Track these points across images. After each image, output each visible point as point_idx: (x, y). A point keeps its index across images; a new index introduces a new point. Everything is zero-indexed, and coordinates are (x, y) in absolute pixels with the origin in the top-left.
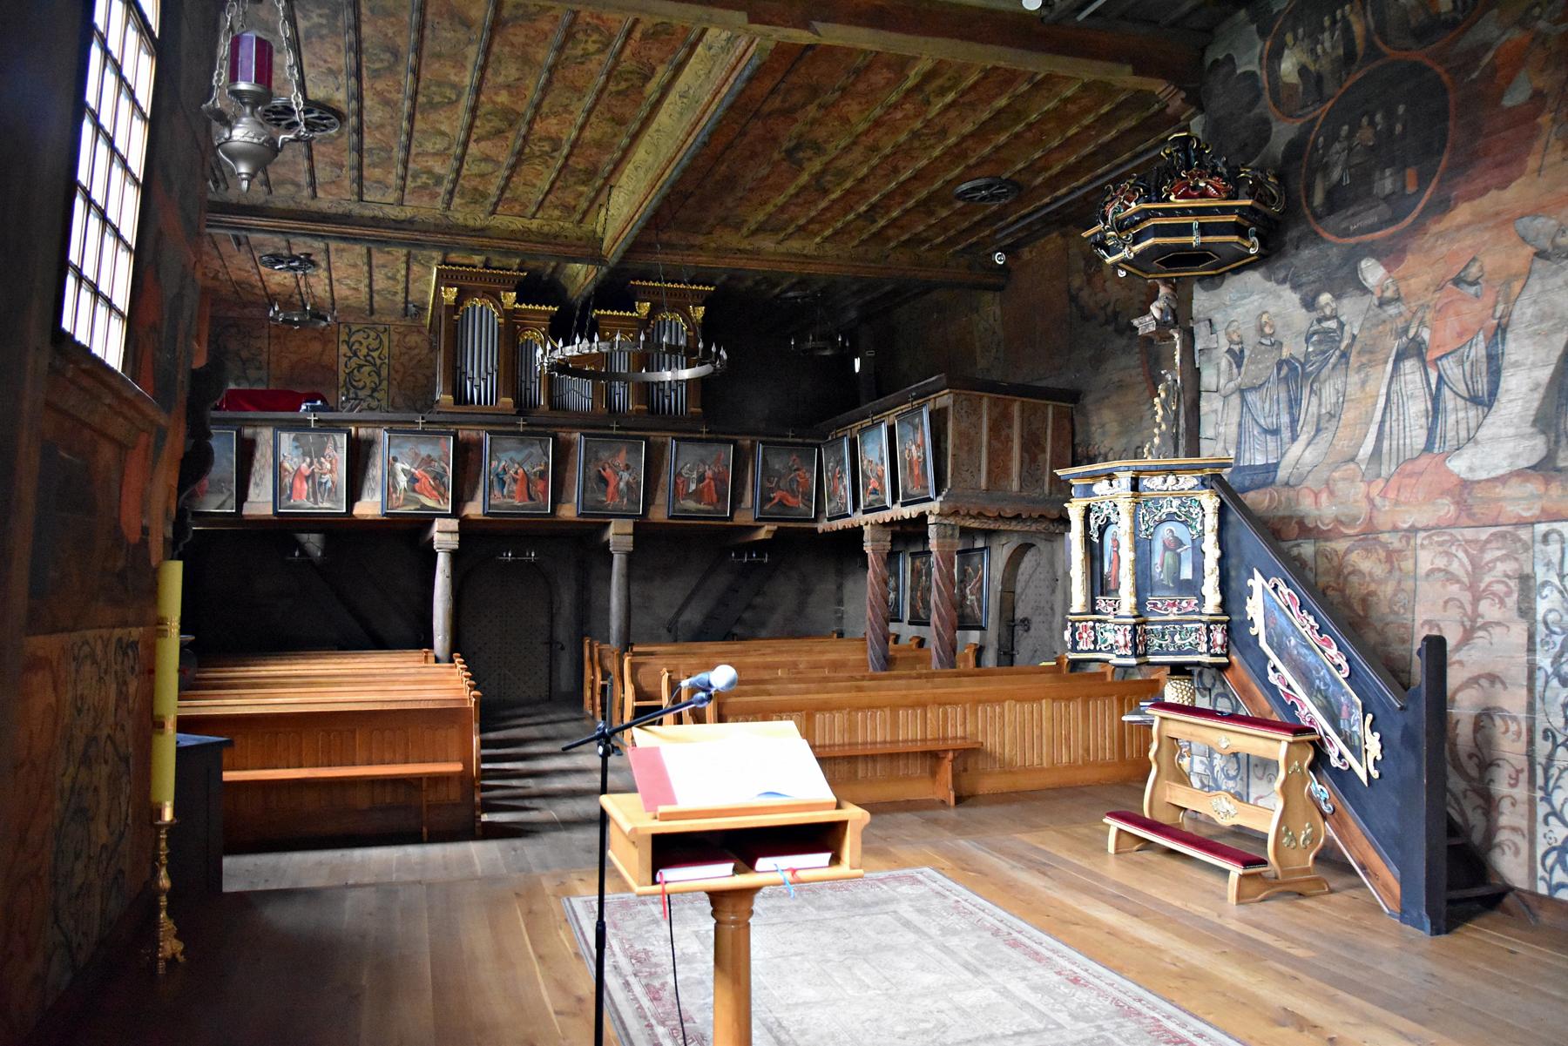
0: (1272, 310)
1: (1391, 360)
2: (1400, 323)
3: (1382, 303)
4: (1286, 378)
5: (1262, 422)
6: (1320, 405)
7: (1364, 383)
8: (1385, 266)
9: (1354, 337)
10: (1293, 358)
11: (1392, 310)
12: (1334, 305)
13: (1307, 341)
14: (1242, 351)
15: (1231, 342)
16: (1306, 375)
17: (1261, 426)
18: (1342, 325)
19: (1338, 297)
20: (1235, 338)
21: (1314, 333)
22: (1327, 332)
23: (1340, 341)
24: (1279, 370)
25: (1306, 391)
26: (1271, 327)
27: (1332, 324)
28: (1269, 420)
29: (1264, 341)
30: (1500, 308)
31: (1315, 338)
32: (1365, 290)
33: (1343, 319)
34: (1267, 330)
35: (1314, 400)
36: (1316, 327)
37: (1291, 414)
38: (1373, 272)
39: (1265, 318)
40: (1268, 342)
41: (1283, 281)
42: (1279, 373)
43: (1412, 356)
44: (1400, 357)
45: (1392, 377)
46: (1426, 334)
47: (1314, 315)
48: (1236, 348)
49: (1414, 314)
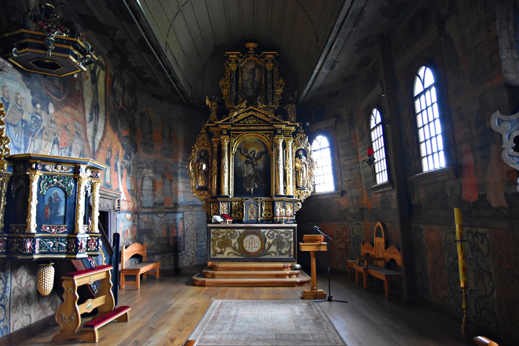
0: (22, 95)
1: (52, 142)
2: (54, 131)
3: (52, 121)
4: (24, 128)
5: (15, 142)
6: (34, 147)
7: (46, 145)
8: (54, 110)
9: (44, 127)
10: (27, 121)
11: (53, 125)
12: (40, 110)
13: (32, 118)
14: (8, 103)
15: (4, 95)
16: (31, 132)
17: (14, 144)
18: (42, 120)
19: (42, 109)
20: (6, 95)
21: (34, 117)
22: (37, 119)
23: (40, 125)
24: (22, 124)
25: (30, 138)
26: (21, 102)
27: (40, 118)
28: (17, 143)
29: (17, 106)
30: (71, 141)
31: (34, 119)
32: (48, 113)
33: (43, 118)
34: (19, 102)
35: (33, 143)
36: (34, 114)
37: (25, 145)
38: (51, 110)
39: (19, 96)
40: (19, 107)
41: (28, 87)
42: (22, 125)
43: (56, 144)
44: (54, 142)
45: (52, 148)
46: (59, 139)
47: (34, 109)
48: (6, 100)
49: (58, 130)
